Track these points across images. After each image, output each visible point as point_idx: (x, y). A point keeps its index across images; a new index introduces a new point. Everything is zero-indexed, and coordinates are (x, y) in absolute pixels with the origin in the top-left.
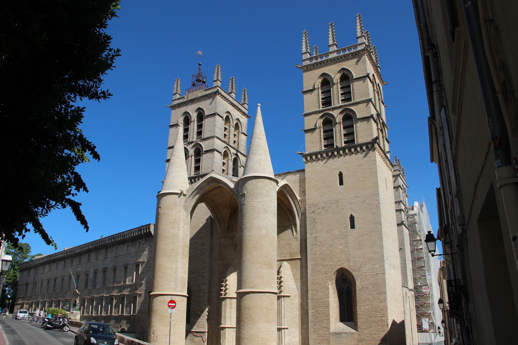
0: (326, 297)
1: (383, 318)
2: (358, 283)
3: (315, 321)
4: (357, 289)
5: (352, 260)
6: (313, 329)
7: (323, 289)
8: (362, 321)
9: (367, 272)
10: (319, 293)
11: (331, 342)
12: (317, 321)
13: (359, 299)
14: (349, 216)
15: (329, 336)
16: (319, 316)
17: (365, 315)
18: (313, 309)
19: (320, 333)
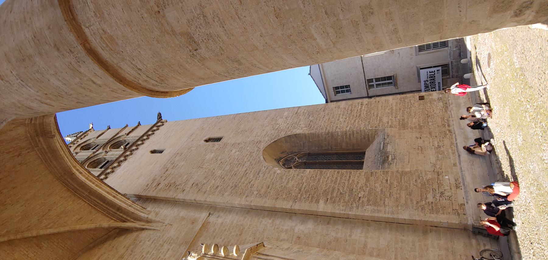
0: (302, 174)
1: (365, 104)
2: (298, 131)
3: (347, 198)
4: (307, 132)
5: (261, 138)
6: (368, 205)
7: (284, 179)
8: (365, 125)
9: (288, 123)
10: (290, 185)
11: (407, 170)
12: (349, 196)
13: (325, 128)
14: (205, 143)
15: (390, 173)
16: (339, 189)
17: (355, 121)
18: (317, 201)
19: (382, 190)
